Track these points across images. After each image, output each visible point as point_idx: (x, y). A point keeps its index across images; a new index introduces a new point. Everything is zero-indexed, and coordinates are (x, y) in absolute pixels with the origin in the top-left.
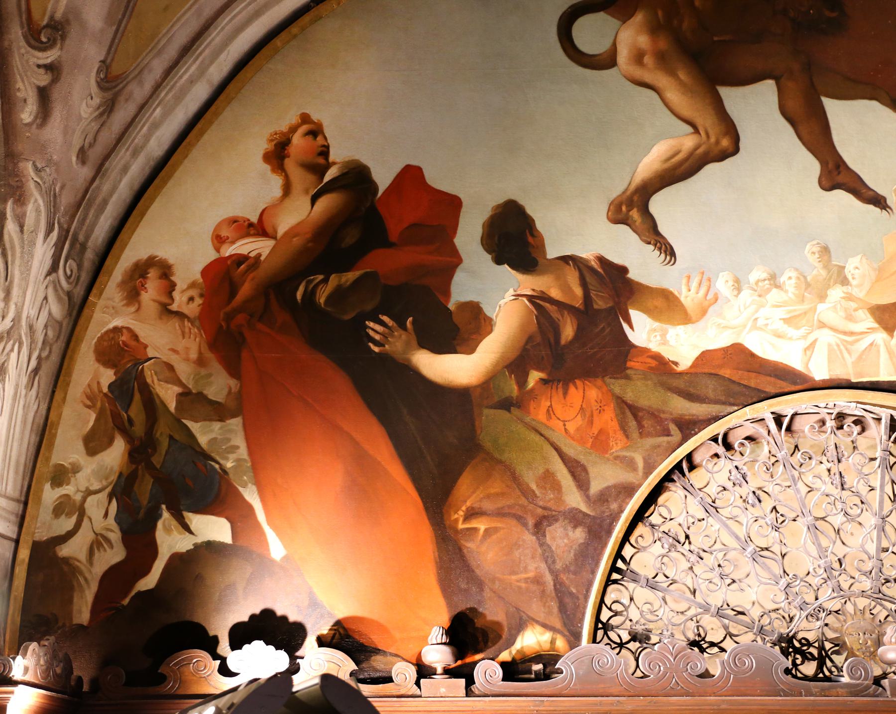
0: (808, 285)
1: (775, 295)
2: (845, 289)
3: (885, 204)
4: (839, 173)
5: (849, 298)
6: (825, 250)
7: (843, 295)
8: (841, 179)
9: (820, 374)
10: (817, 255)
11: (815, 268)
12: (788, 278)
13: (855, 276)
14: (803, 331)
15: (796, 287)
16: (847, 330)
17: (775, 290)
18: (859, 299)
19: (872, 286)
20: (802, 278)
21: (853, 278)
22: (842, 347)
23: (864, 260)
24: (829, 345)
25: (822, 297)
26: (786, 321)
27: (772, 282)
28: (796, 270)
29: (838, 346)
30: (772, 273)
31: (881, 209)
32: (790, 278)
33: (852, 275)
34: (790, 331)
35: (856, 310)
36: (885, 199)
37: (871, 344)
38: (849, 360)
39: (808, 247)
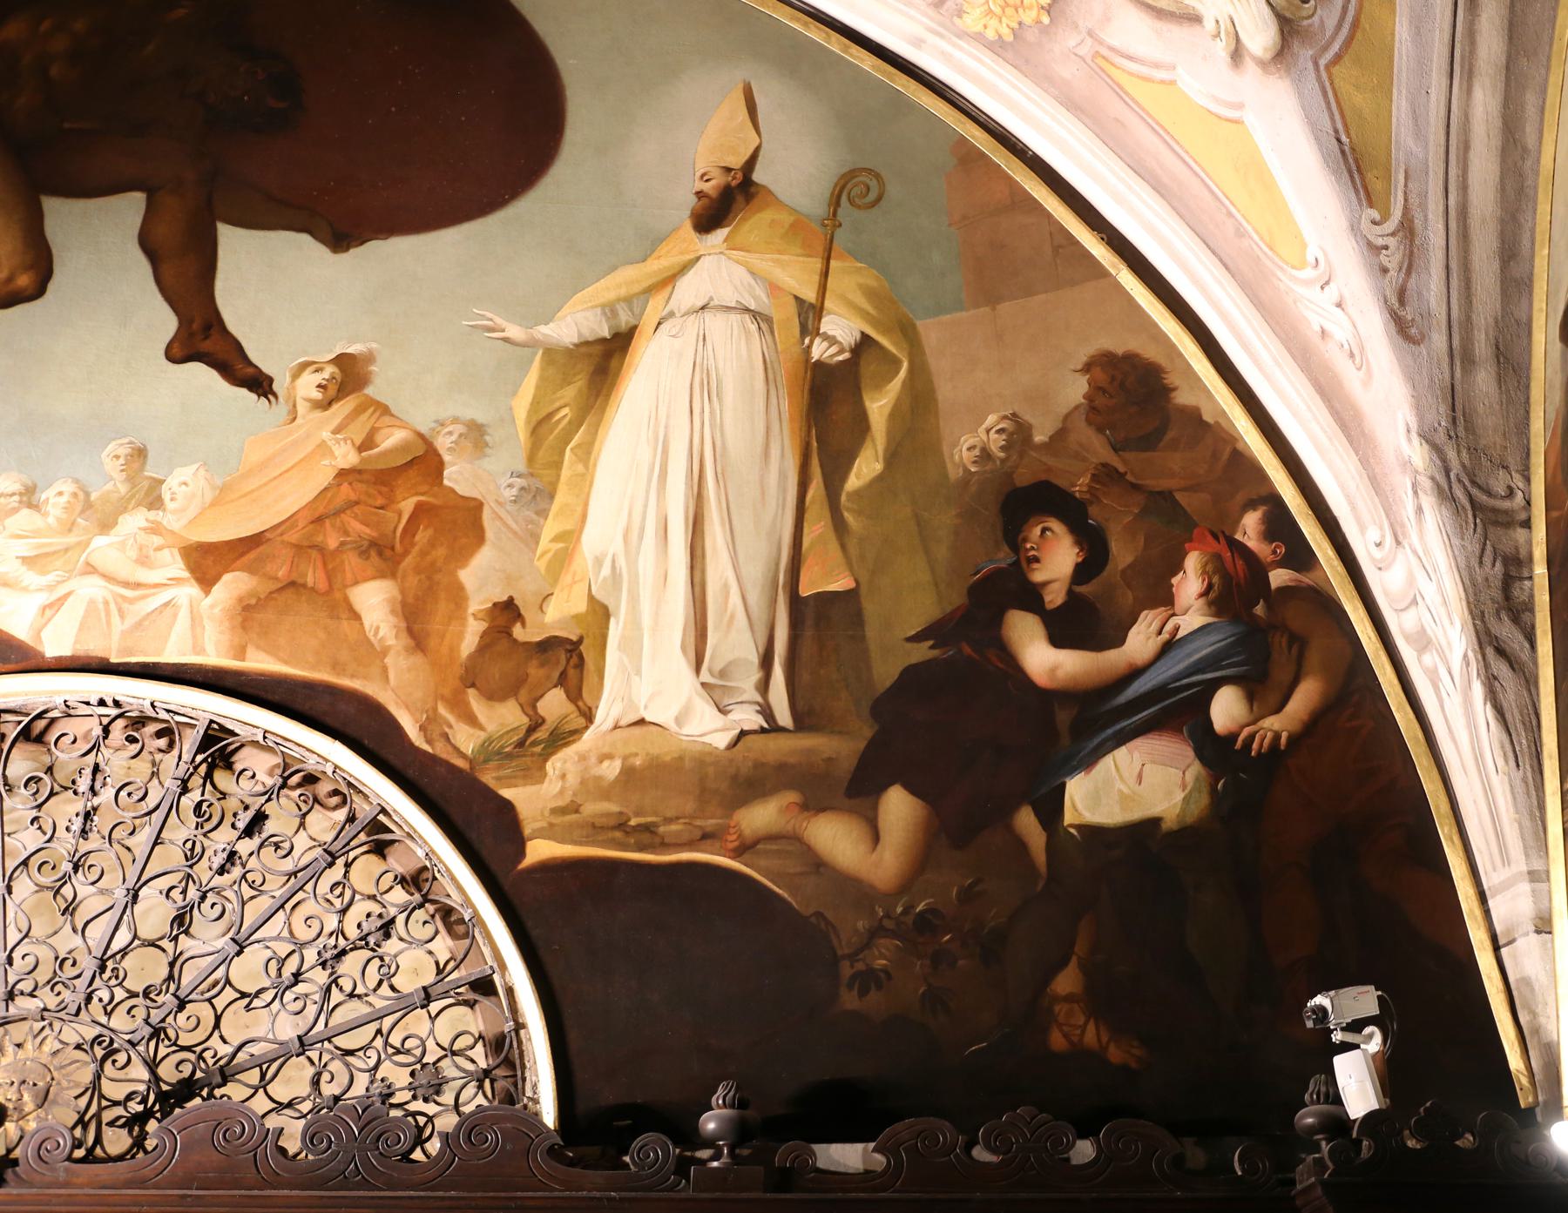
0: (88, 505)
1: (25, 519)
2: (152, 515)
3: (267, 389)
4: (206, 338)
5: (155, 529)
6: (140, 453)
7: (145, 524)
8: (207, 346)
9: (54, 647)
10: (122, 461)
11: (112, 479)
12: (57, 497)
13: (177, 496)
14: (51, 578)
15: (65, 508)
16: (132, 579)
17: (25, 511)
18: (172, 532)
19: (200, 513)
20: (81, 495)
21: (172, 500)
22: (113, 606)
23: (202, 472)
24: (92, 602)
25: (106, 526)
26: (25, 560)
27: (25, 499)
28: (76, 481)
29: (106, 603)
30: (30, 484)
31: (259, 396)
32: (60, 494)
33: (173, 493)
34: (31, 578)
35: (159, 549)
36: (270, 380)
37: (166, 604)
38: (118, 626)
39: (110, 447)
